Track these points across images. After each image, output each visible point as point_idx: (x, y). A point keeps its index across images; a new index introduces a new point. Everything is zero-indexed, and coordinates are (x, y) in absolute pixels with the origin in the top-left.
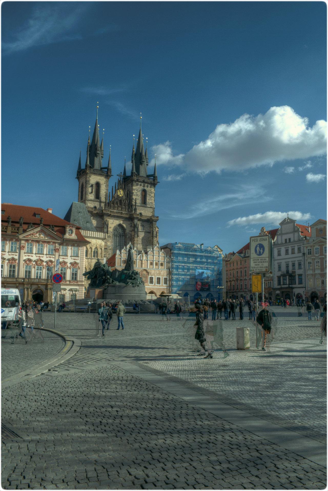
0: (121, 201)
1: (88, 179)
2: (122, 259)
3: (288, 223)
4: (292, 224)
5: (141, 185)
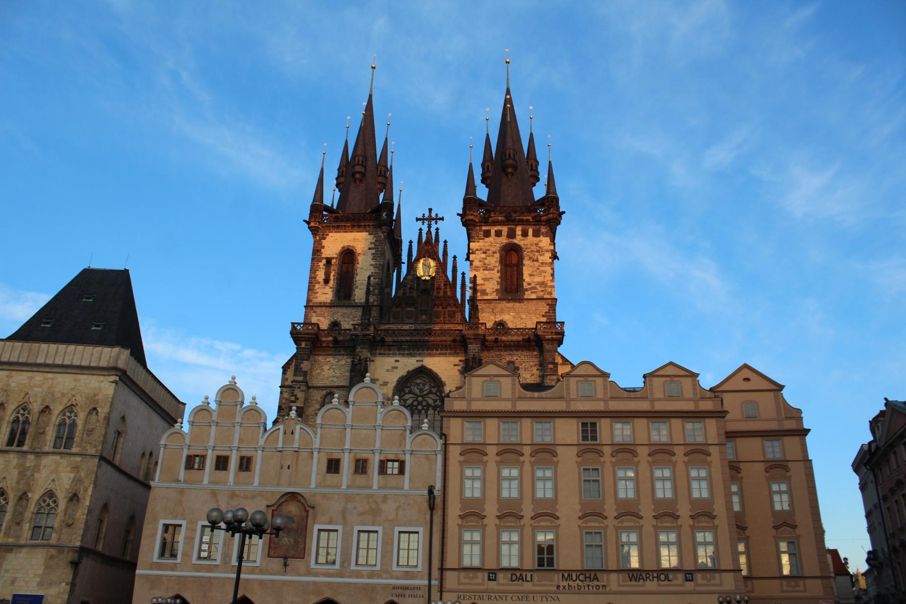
5: (498, 234)
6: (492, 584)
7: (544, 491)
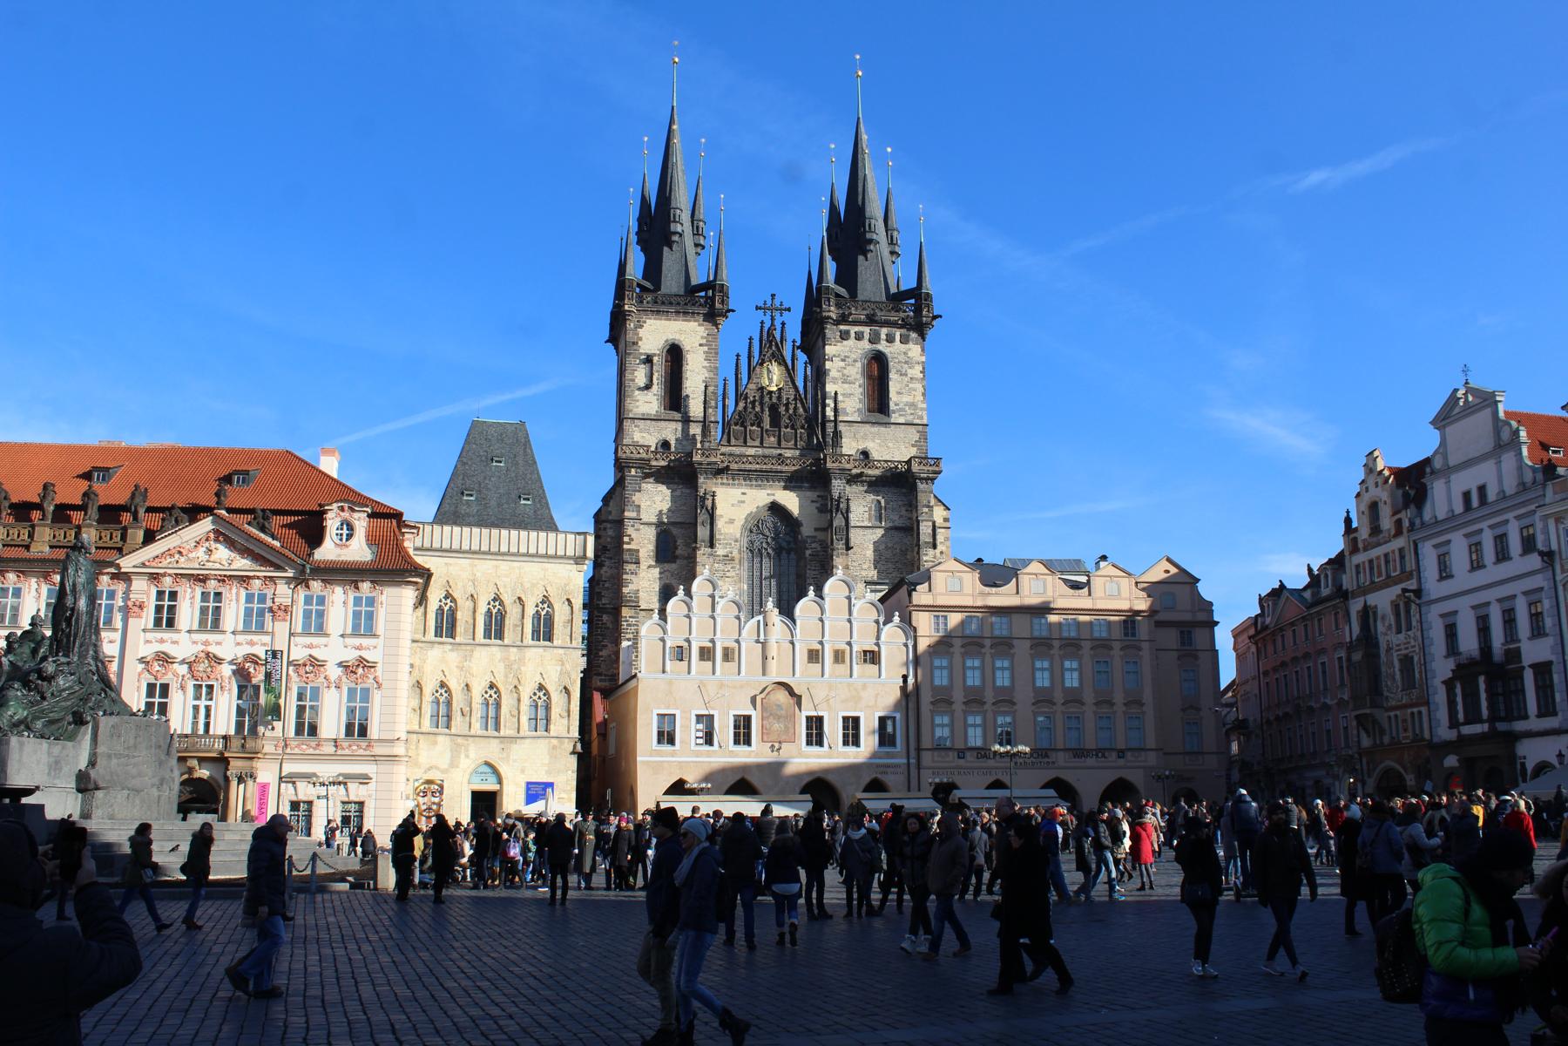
0: (774, 409)
1: (630, 337)
2: (669, 644)
3: (1469, 410)
4: (1488, 411)
5: (859, 337)
6: (961, 762)
7: (1003, 679)
